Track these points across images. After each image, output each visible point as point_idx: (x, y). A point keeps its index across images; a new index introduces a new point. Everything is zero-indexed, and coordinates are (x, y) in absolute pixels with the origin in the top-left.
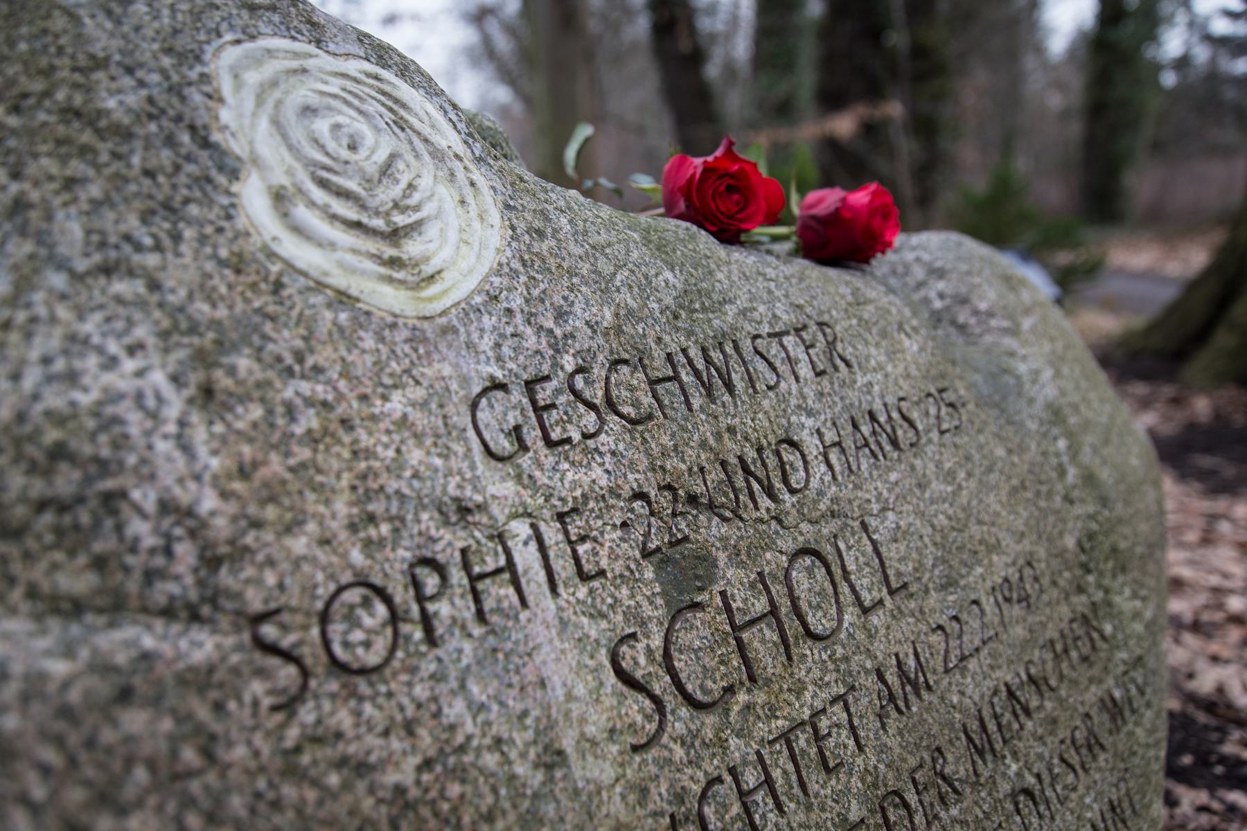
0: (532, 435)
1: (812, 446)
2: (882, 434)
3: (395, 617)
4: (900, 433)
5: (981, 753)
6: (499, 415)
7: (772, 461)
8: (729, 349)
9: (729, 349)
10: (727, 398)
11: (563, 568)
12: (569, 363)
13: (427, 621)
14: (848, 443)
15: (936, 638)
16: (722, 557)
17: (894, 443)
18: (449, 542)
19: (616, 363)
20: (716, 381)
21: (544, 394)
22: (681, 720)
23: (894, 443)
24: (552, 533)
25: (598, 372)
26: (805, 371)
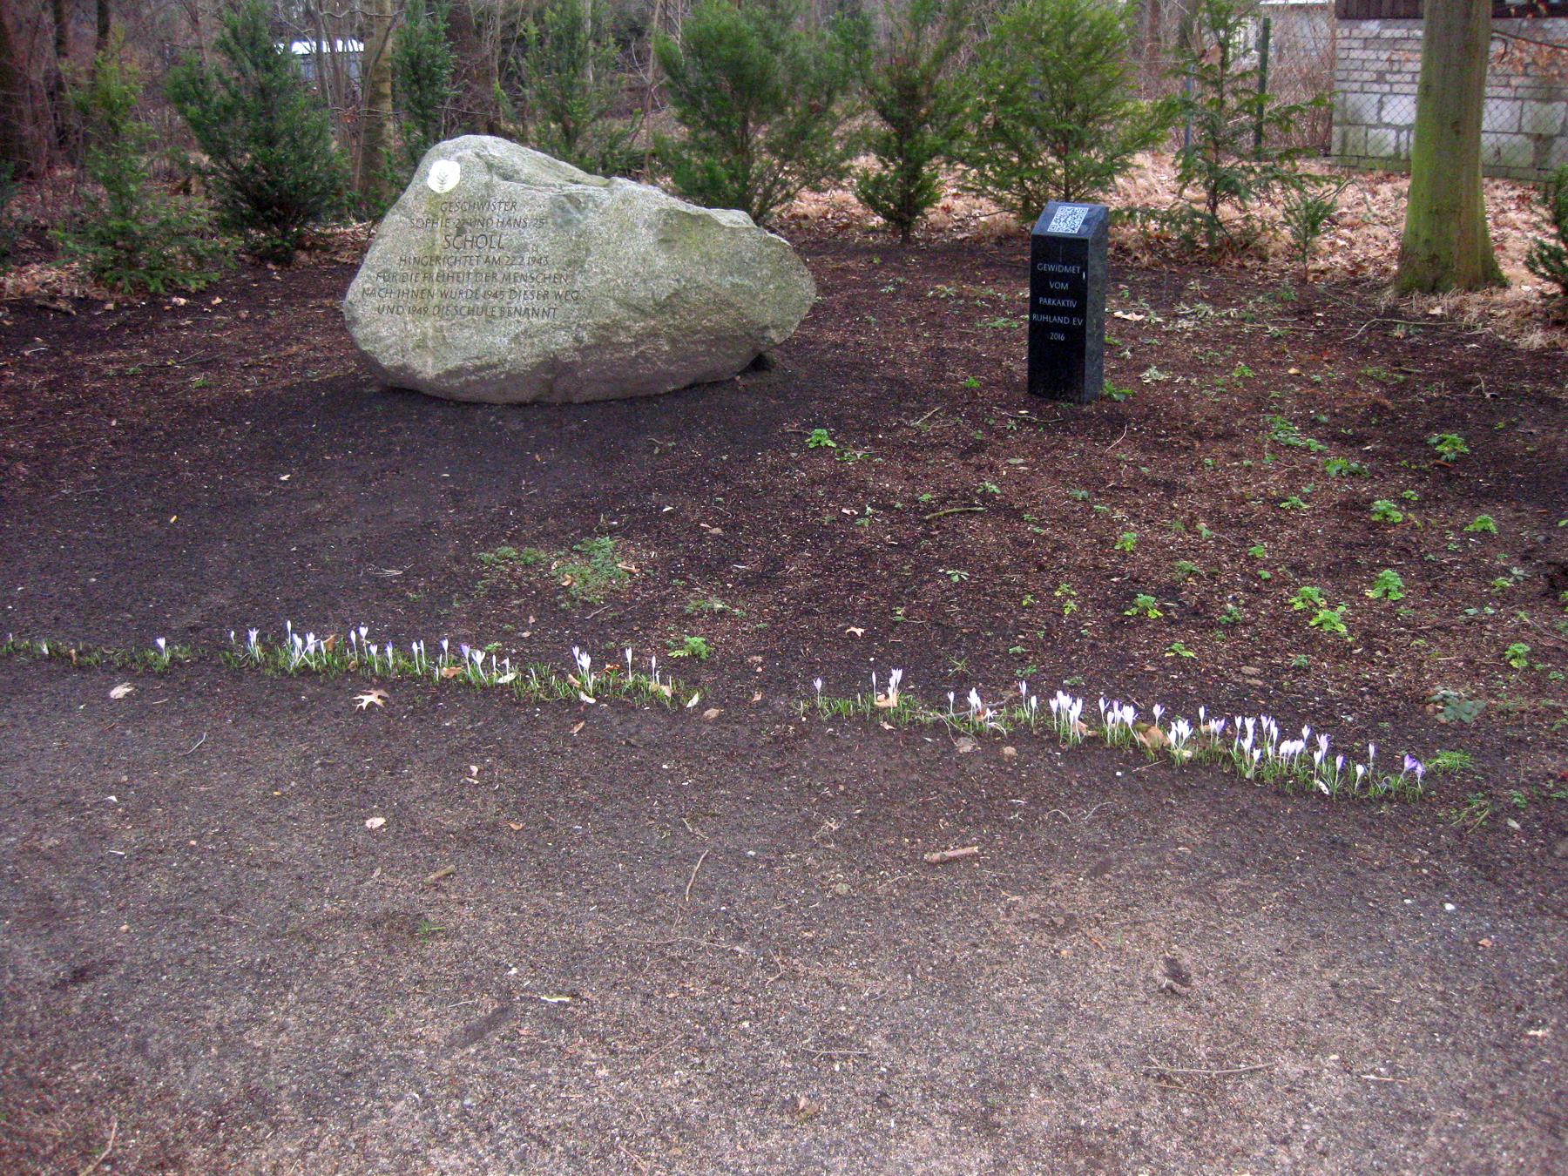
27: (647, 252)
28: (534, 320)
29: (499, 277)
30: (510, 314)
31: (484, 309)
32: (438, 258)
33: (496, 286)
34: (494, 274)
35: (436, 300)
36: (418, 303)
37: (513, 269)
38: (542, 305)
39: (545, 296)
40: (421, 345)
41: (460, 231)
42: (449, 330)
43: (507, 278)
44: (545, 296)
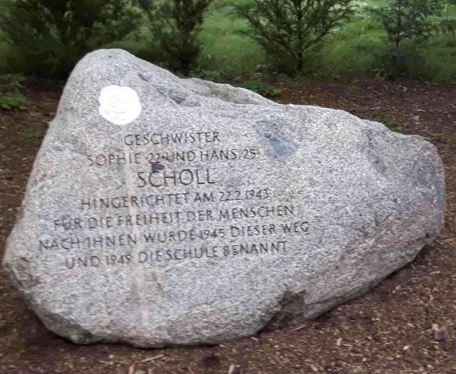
0: (135, 143)
1: (198, 154)
2: (224, 155)
3: (106, 160)
4: (229, 156)
5: (224, 216)
6: (128, 140)
7: (186, 155)
8: (183, 135)
9: (183, 135)
10: (178, 143)
11: (133, 161)
12: (145, 133)
13: (110, 162)
14: (210, 155)
15: (219, 194)
16: (166, 167)
17: (227, 157)
18: (116, 153)
19: (155, 134)
20: (177, 140)
21: (138, 137)
22: (148, 186)
23: (227, 157)
24: (133, 156)
25: (150, 135)
26: (203, 141)
27: (369, 178)
28: (263, 255)
29: (215, 214)
30: (235, 253)
31: (204, 250)
32: (134, 199)
33: (212, 225)
34: (209, 212)
35: (141, 246)
36: (118, 251)
37: (228, 206)
38: (272, 238)
39: (272, 229)
40: (133, 299)
41: (156, 167)
42: (166, 277)
43: (224, 214)
44: (272, 229)
